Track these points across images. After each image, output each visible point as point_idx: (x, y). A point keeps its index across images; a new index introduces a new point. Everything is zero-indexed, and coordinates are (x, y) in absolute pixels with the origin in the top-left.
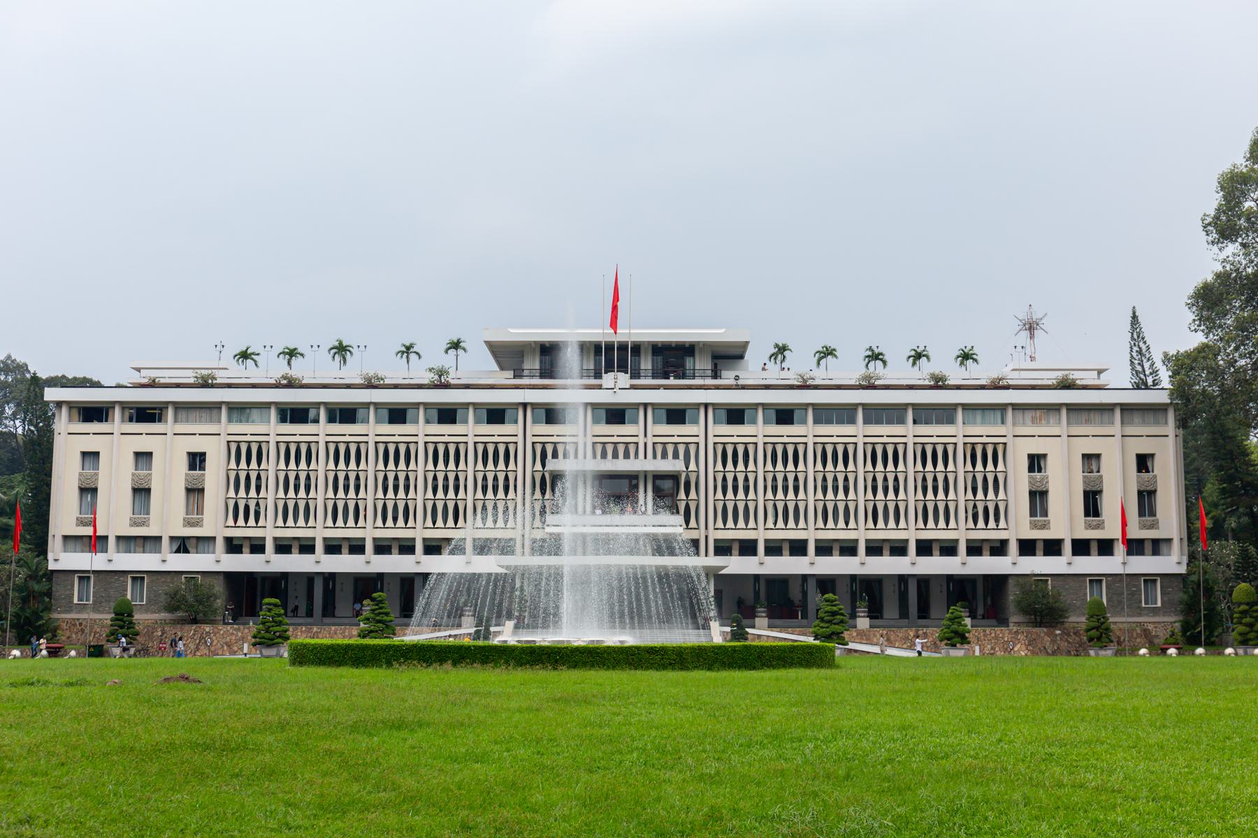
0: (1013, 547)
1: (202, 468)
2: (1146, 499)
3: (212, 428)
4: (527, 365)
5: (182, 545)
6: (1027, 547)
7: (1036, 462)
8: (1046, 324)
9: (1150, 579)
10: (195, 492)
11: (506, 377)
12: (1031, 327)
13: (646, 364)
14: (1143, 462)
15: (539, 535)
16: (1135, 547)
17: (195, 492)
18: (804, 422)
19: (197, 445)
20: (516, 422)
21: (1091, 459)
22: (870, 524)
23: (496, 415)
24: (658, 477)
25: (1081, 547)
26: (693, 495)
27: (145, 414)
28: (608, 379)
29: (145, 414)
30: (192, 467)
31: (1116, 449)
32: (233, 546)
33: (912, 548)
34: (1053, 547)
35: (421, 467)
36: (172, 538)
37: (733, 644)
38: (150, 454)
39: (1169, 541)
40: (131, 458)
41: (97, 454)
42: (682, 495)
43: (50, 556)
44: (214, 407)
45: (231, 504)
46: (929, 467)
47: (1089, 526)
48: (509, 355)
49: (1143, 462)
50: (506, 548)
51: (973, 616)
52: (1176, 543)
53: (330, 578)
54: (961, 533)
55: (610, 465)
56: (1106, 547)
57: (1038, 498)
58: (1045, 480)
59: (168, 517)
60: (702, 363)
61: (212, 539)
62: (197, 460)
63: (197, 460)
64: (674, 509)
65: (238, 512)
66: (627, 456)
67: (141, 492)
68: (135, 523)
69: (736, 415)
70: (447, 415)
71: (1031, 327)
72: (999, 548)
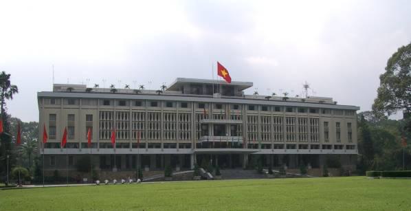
0: (321, 147)
1: (91, 120)
2: (350, 134)
3: (95, 107)
4: (185, 90)
5: (85, 145)
6: (324, 147)
7: (326, 123)
8: (310, 86)
9: (351, 156)
10: (89, 128)
11: (180, 93)
12: (306, 87)
13: (221, 90)
14: (349, 124)
15: (199, 142)
16: (348, 147)
17: (89, 128)
18: (283, 111)
19: (90, 112)
20: (191, 107)
21: (338, 124)
22: (149, 138)
23: (184, 105)
24: (232, 125)
25: (336, 147)
26: (241, 131)
27: (72, 101)
28: (216, 95)
29: (72, 101)
30: (87, 119)
31: (343, 120)
32: (103, 146)
33: (298, 147)
34: (329, 147)
35: (163, 120)
36: (82, 143)
37: (182, 172)
38: (73, 115)
39: (354, 146)
40: (48, 116)
41: (55, 115)
42: (238, 131)
43: (41, 149)
44: (96, 99)
45: (101, 132)
46: (168, 120)
47: (338, 142)
48: (181, 86)
49: (349, 124)
50: (188, 146)
51: (288, 165)
52: (356, 147)
53: (134, 156)
54: (309, 142)
55: (201, 121)
56: (341, 147)
57: (327, 133)
58: (328, 129)
59: (80, 136)
60: (236, 92)
61: (97, 143)
62: (89, 117)
63: (89, 117)
64: (239, 135)
65: (102, 134)
66: (222, 118)
67: (71, 127)
68: (69, 138)
69: (252, 107)
70: (169, 104)
71: (306, 87)
72: (317, 147)
